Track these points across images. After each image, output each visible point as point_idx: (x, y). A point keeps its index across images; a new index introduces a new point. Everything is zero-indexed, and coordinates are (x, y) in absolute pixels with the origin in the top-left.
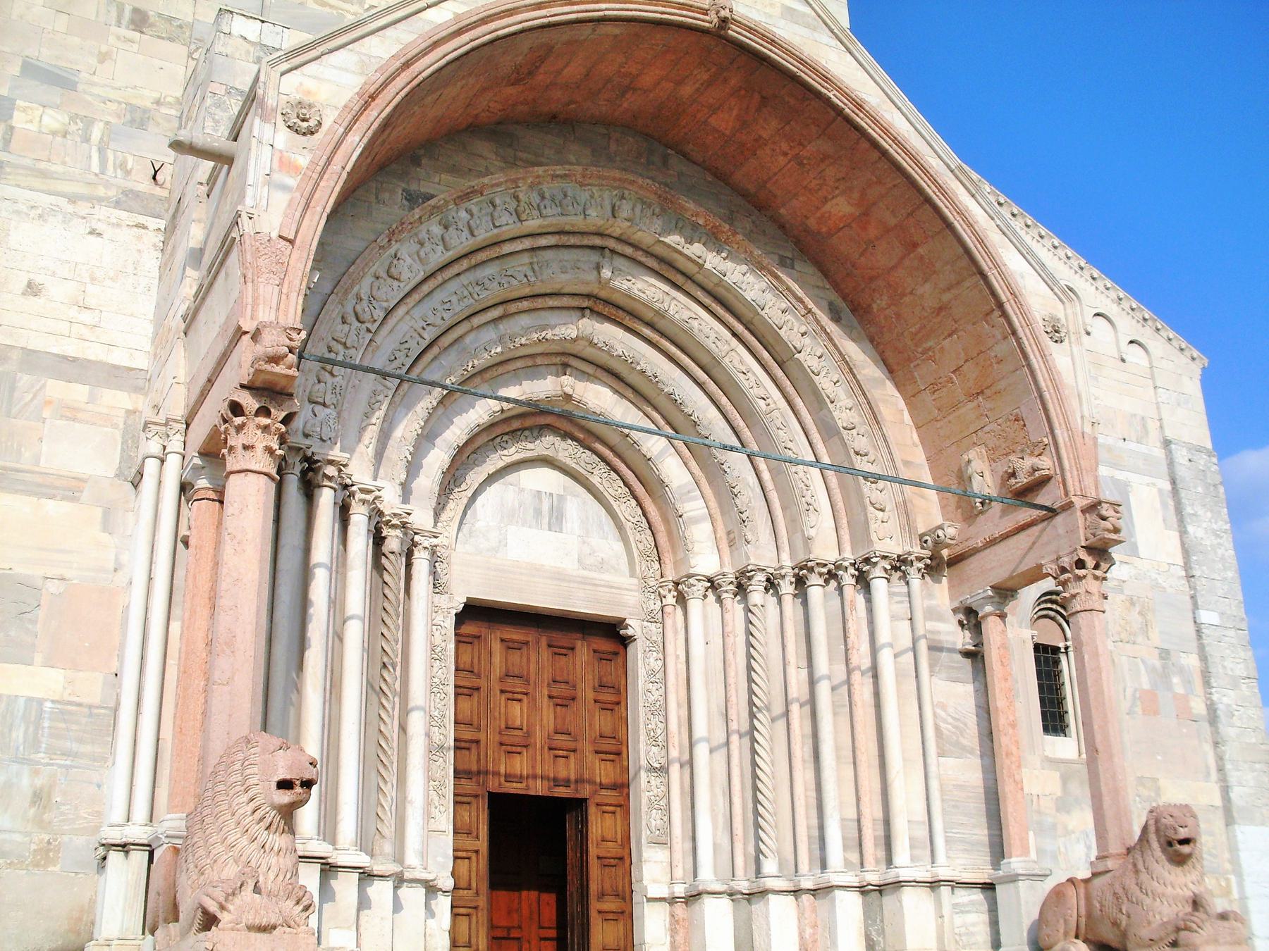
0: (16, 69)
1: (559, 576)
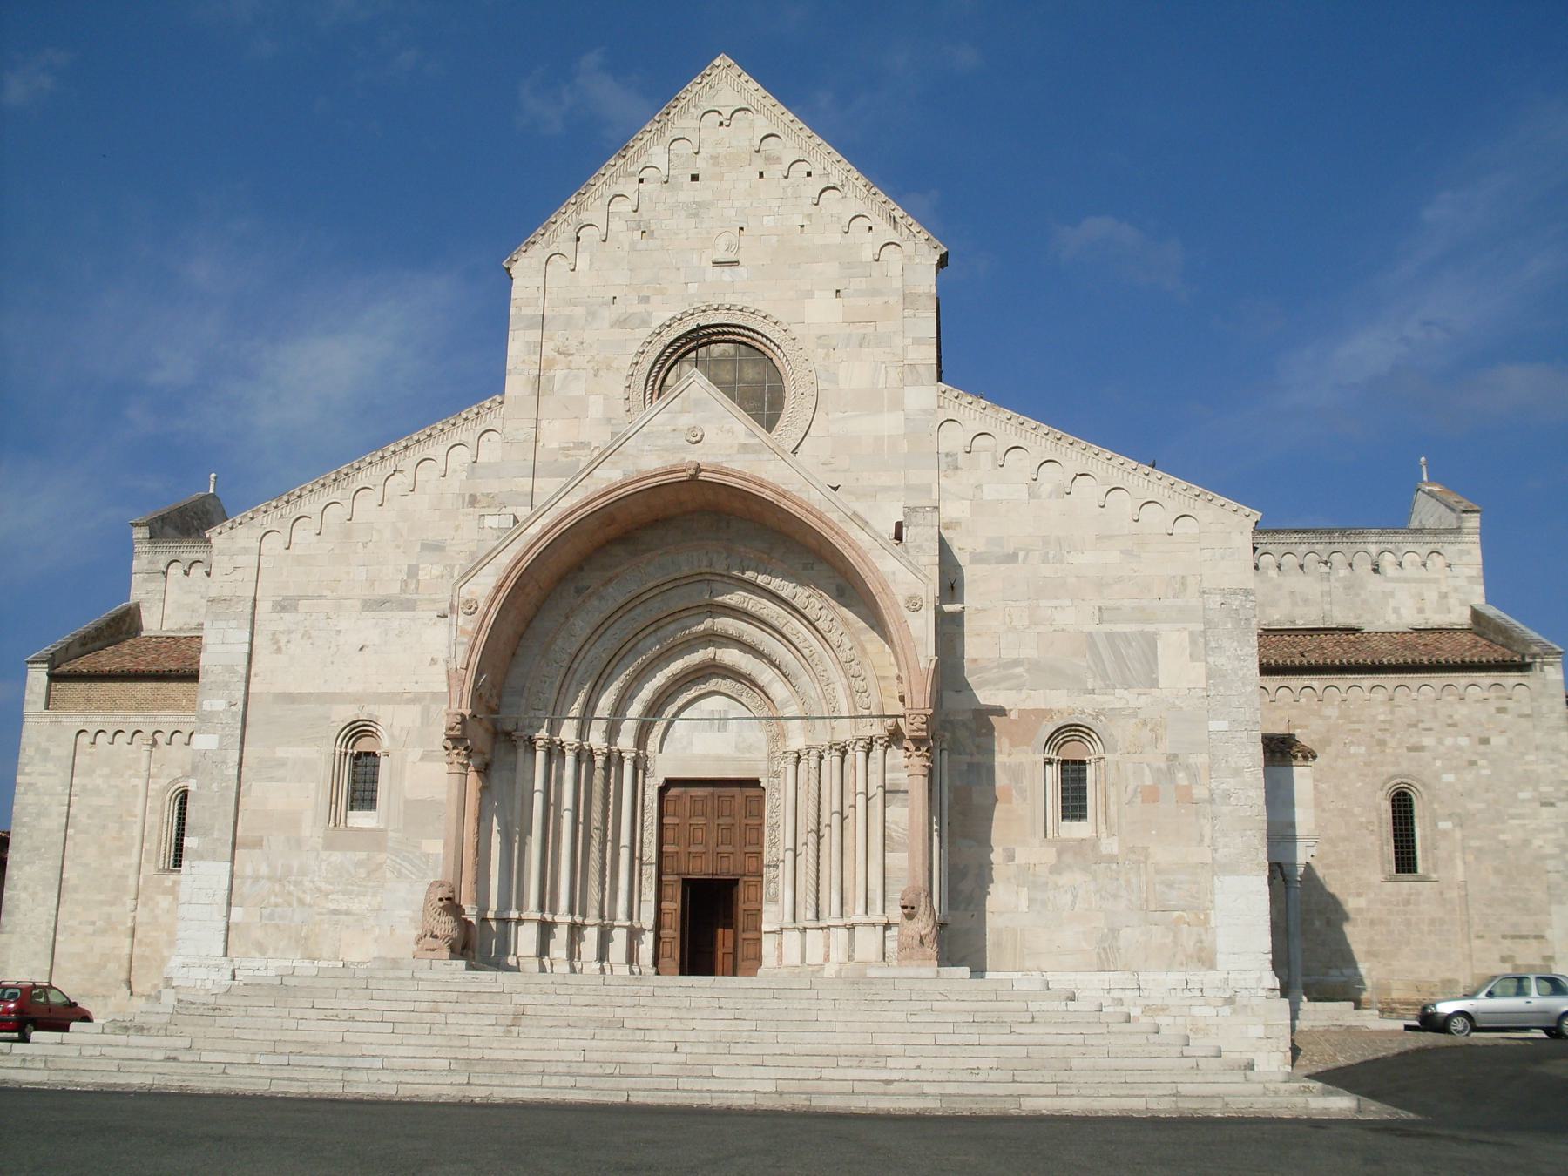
0: (418, 549)
1: (718, 759)
